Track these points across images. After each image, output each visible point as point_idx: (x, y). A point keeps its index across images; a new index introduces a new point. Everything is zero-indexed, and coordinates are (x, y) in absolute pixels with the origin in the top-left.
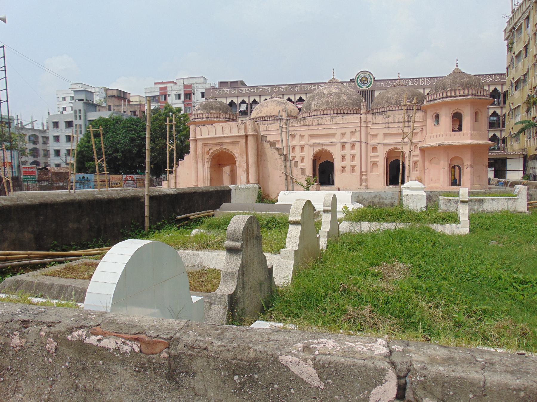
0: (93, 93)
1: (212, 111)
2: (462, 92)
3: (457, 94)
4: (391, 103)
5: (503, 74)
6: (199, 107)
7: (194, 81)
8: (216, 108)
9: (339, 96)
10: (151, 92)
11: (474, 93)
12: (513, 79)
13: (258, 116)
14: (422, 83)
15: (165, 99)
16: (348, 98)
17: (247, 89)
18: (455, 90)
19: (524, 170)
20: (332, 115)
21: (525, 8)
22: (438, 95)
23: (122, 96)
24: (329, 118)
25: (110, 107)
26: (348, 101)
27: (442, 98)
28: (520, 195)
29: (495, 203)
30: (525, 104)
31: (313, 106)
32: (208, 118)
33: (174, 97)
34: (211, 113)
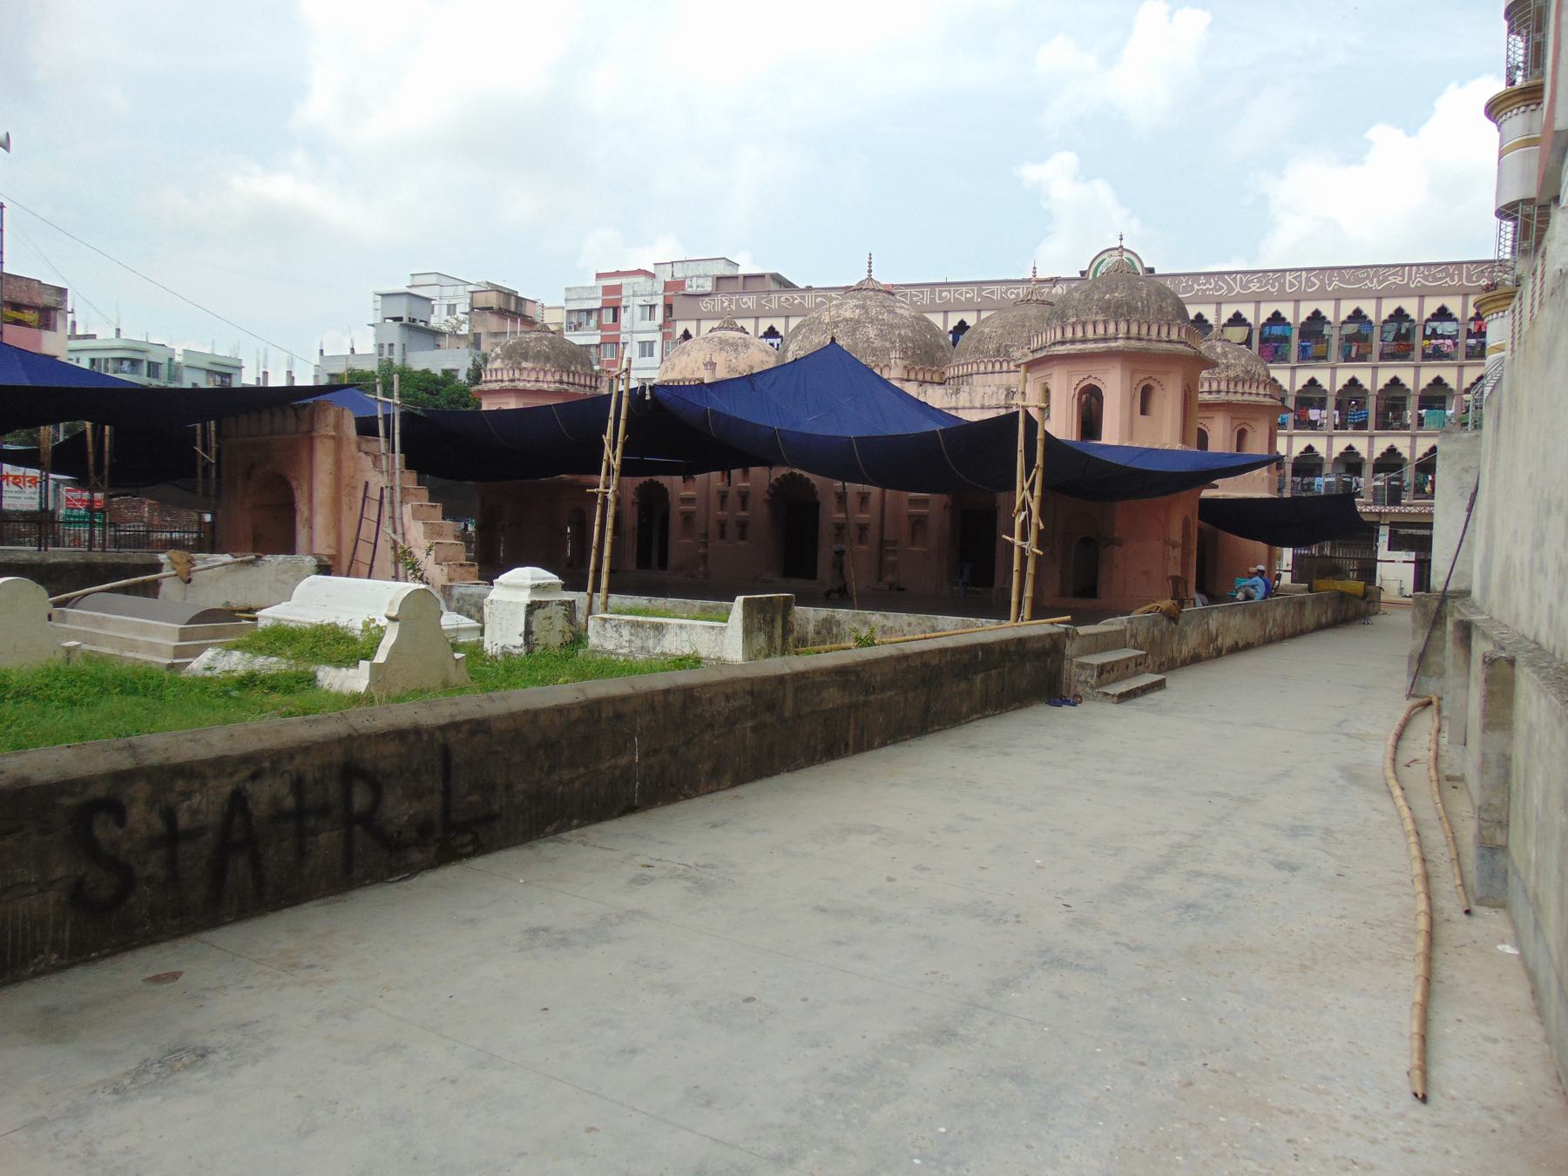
0: (429, 300)
1: (524, 364)
3: (1090, 334)
4: (986, 353)
8: (538, 356)
9: (855, 330)
10: (580, 299)
11: (1134, 330)
14: (1292, 285)
15: (615, 318)
16: (881, 335)
18: (1084, 325)
23: (511, 308)
25: (477, 336)
26: (877, 343)
29: (685, 635)
33: (638, 311)
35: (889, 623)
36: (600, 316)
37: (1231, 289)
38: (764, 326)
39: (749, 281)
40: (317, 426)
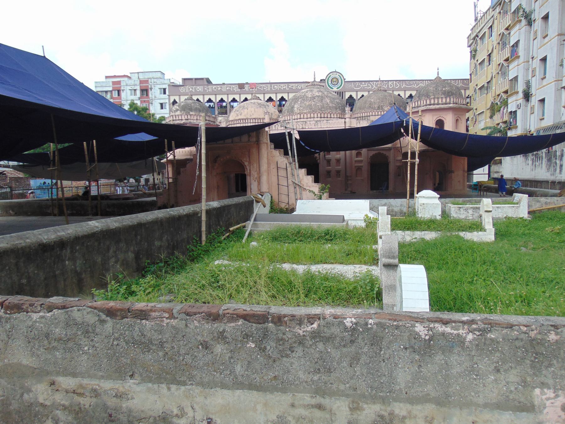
2: (444, 101)
3: (440, 102)
4: (374, 109)
5: (465, 79)
6: (177, 108)
7: (151, 75)
9: (322, 100)
10: (101, 86)
12: (477, 85)
13: (237, 118)
14: (391, 86)
15: (119, 95)
16: (331, 102)
17: (214, 87)
18: (438, 98)
19: (489, 174)
20: (316, 119)
21: (489, 18)
22: (422, 102)
24: (314, 122)
26: (331, 105)
27: (426, 105)
28: (522, 203)
30: (489, 111)
31: (295, 109)
32: (187, 120)
33: (129, 92)
34: (191, 115)
35: (548, 201)
36: (112, 94)
37: (372, 87)
38: (267, 97)
39: (197, 81)
40: (261, 139)
